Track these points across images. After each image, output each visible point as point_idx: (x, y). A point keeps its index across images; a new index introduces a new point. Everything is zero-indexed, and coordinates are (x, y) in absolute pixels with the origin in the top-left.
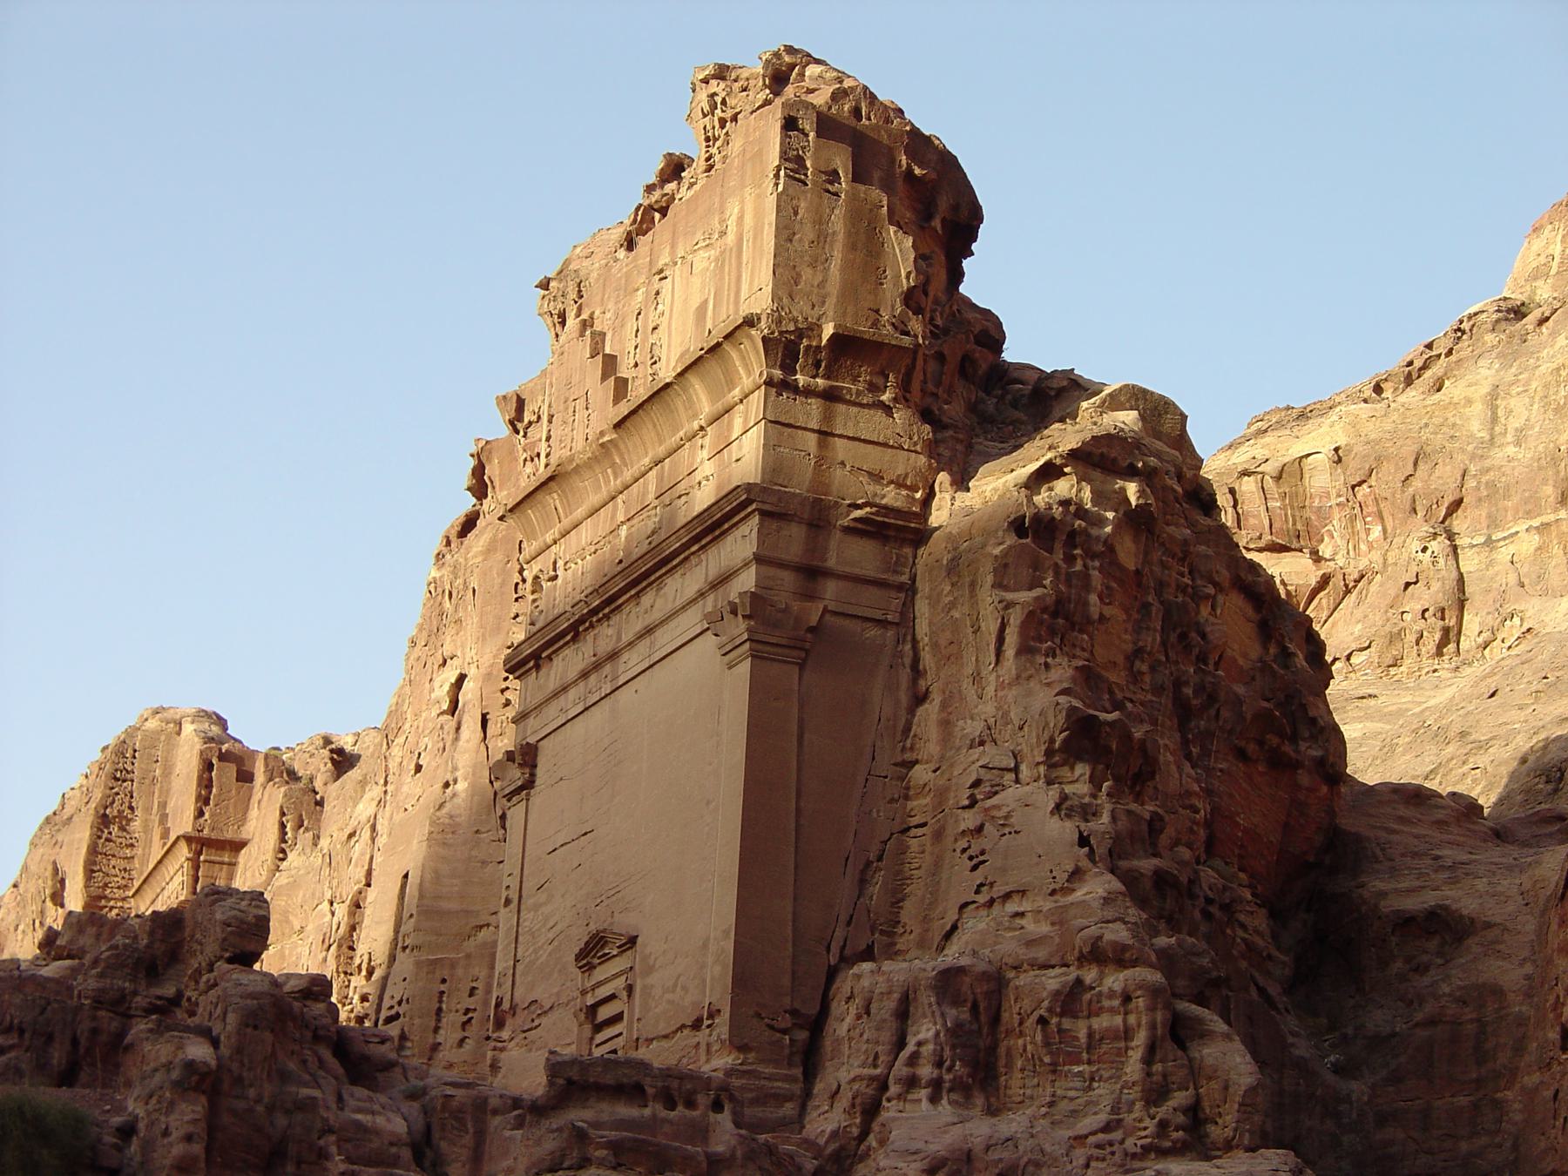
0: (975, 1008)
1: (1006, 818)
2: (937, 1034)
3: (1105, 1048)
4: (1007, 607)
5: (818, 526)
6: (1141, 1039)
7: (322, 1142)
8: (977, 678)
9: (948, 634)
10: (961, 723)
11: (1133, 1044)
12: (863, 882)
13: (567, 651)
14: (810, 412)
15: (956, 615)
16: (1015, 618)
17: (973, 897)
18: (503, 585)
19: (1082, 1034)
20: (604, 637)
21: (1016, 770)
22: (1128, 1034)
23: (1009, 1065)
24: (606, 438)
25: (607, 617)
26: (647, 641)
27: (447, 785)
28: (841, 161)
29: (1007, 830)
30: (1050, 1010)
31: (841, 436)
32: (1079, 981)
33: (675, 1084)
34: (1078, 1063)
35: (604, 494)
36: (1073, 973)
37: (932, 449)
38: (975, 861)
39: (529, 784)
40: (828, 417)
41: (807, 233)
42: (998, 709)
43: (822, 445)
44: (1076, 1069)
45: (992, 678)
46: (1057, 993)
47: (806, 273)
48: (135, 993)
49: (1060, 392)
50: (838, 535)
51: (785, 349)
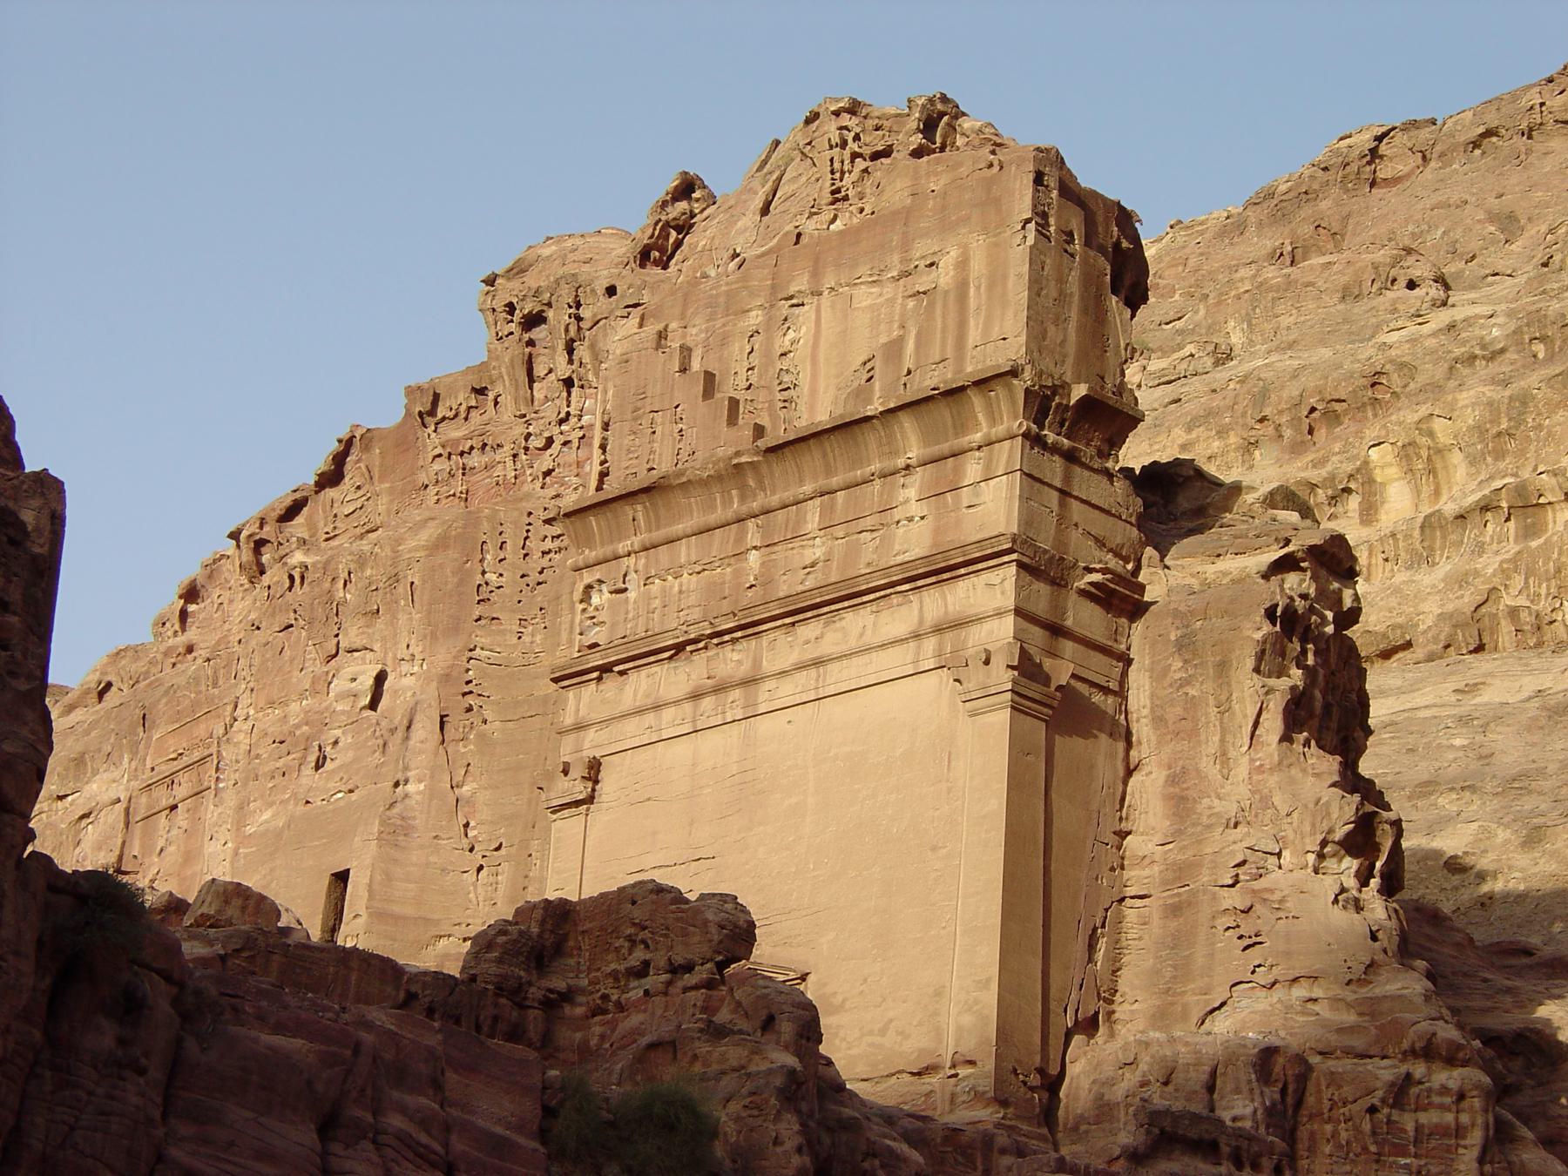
0: (1283, 1091)
1: (1280, 902)
2: (1255, 1111)
3: (1433, 1143)
4: (1267, 693)
5: (1059, 585)
6: (1476, 1138)
7: (866, 1165)
8: (1223, 757)
9: (1179, 710)
10: (1206, 801)
11: (1467, 1142)
12: (1092, 947)
13: (655, 669)
14: (1054, 469)
15: (1192, 692)
16: (1276, 706)
17: (1249, 977)
18: (461, 583)
19: (1410, 1127)
20: (732, 660)
21: (1279, 855)
22: (1460, 1132)
23: (1312, 1150)
24: (744, 459)
25: (734, 641)
26: (813, 672)
27: (397, 784)
28: (1076, 225)
29: (1282, 914)
30: (1383, 1101)
31: (1076, 498)
32: (1408, 1076)
33: (1245, 1144)
34: (1405, 1155)
35: (730, 514)
36: (1403, 1069)
37: (1142, 522)
38: (1247, 942)
39: (590, 800)
40: (1067, 478)
41: (1051, 290)
42: (1253, 792)
43: (1062, 504)
44: (1403, 1161)
45: (1246, 759)
46: (1392, 1084)
47: (1052, 330)
48: (530, 984)
49: (1188, 479)
50: (1073, 596)
51: (1040, 404)
